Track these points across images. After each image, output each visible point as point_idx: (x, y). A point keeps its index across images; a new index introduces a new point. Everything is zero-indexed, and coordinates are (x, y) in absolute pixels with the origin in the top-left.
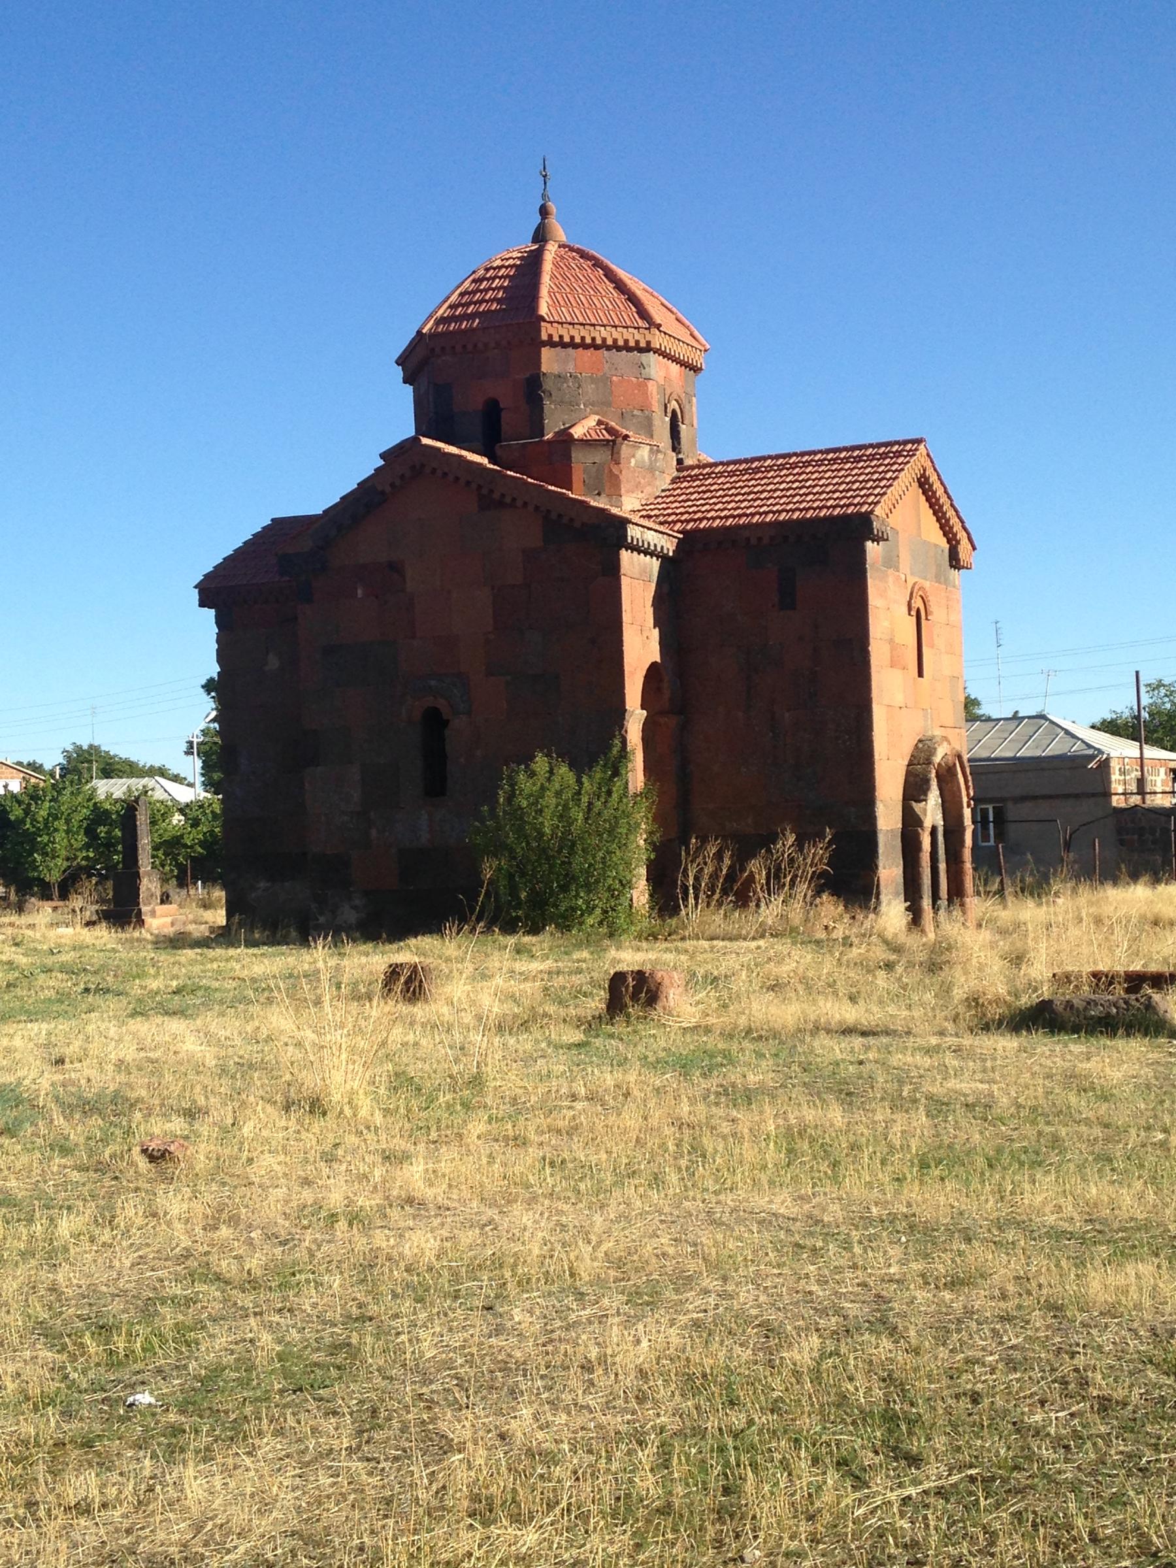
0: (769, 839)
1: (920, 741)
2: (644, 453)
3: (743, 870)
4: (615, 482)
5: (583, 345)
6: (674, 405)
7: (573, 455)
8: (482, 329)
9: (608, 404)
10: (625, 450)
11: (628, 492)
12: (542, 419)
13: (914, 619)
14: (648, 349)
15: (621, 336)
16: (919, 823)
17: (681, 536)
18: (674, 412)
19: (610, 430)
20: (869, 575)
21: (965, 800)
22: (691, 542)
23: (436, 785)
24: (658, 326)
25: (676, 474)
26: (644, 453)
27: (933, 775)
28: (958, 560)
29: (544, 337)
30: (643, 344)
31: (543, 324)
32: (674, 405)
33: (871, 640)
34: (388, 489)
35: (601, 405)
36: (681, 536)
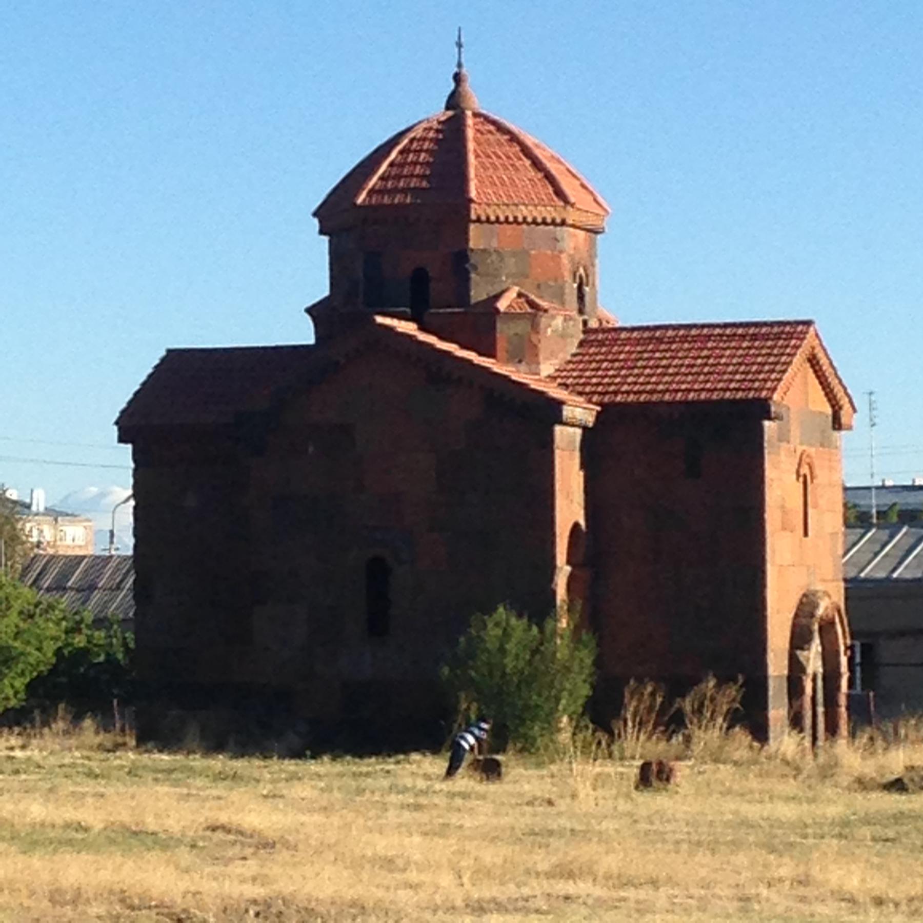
0: (697, 681)
1: (805, 595)
2: (558, 322)
3: (671, 705)
7: (499, 325)
10: (544, 321)
11: (547, 359)
12: (468, 290)
13: (801, 486)
14: (563, 223)
15: (540, 213)
16: (803, 670)
17: (599, 408)
18: (581, 278)
19: (532, 304)
20: (766, 451)
22: (609, 415)
23: (378, 623)
24: (573, 205)
25: (582, 336)
26: (558, 322)
27: (816, 627)
29: (473, 216)
30: (558, 221)
31: (473, 205)
32: (581, 271)
33: (767, 509)
34: (343, 361)
35: (521, 276)
36: (599, 408)
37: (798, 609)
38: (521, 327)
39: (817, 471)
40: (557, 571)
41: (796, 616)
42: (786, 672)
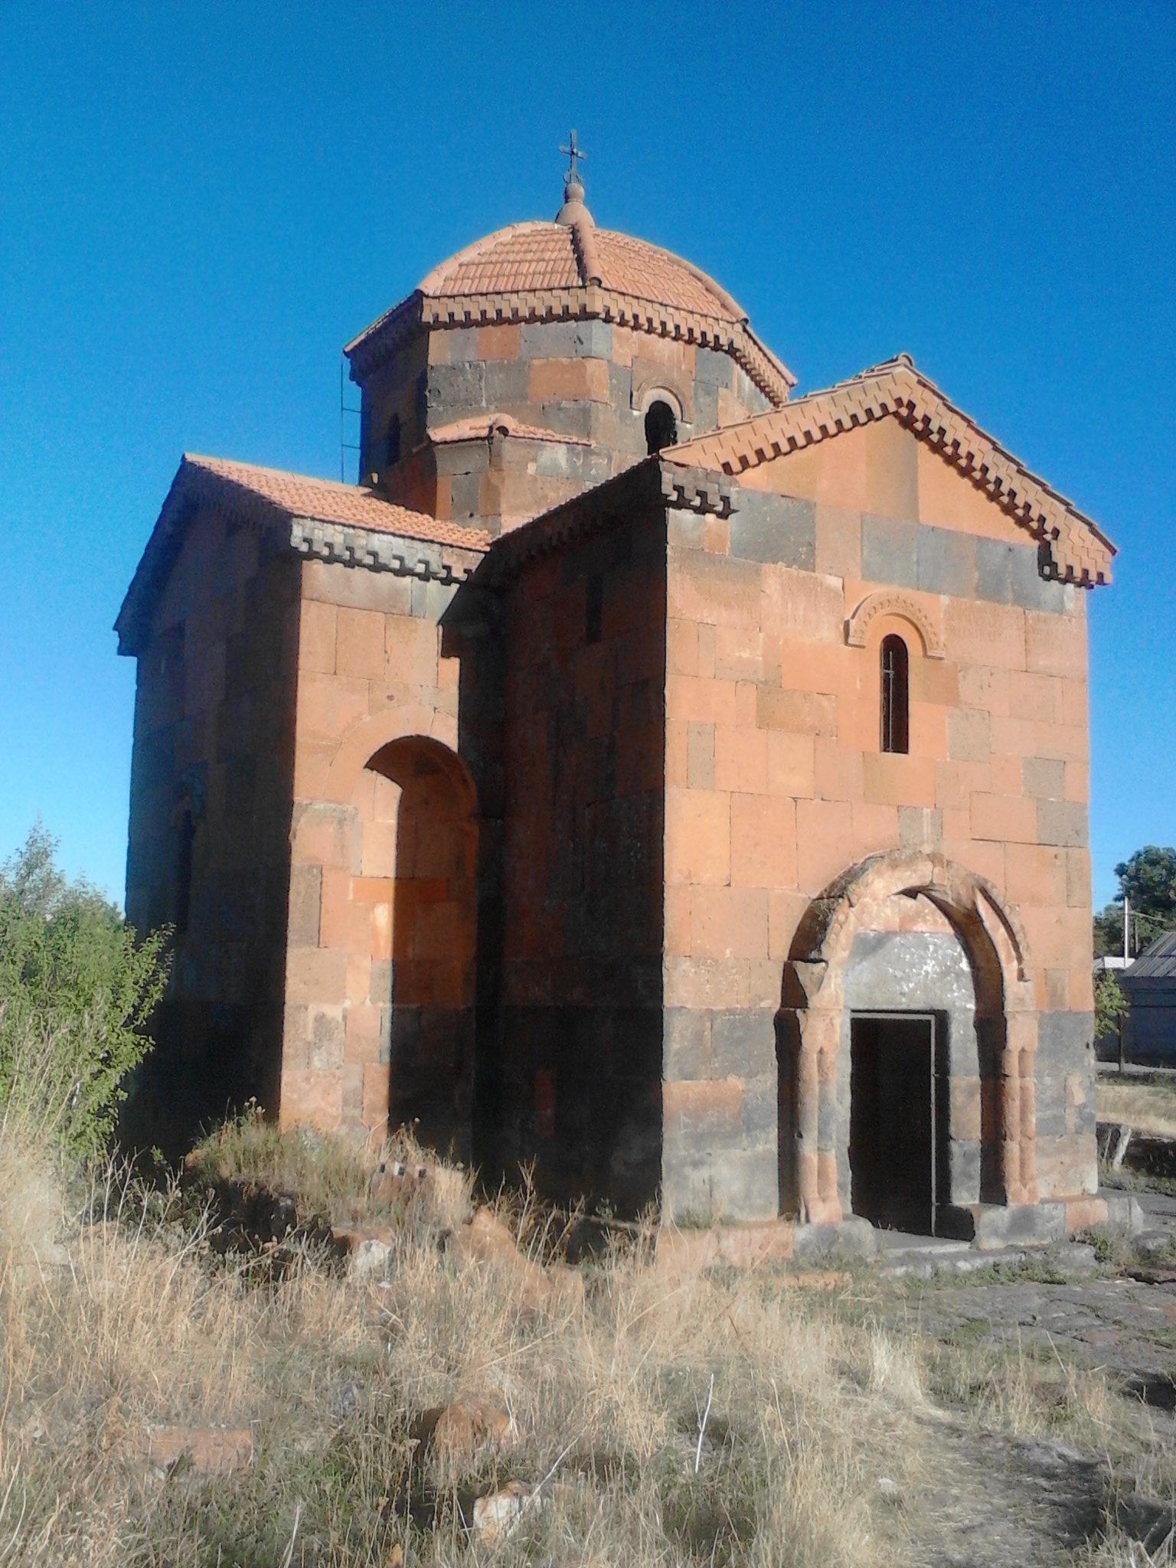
2: (558, 455)
4: (493, 494)
5: (484, 322)
6: (651, 396)
7: (439, 464)
8: (385, 327)
9: (524, 397)
10: (507, 447)
11: (515, 509)
14: (586, 315)
17: (488, 549)
20: (671, 567)
21: (1010, 971)
28: (1054, 566)
29: (427, 317)
30: (575, 309)
31: (425, 301)
33: (668, 677)
37: (833, 885)
38: (475, 460)
39: (940, 637)
40: (295, 813)
41: (821, 898)
42: (772, 1003)
